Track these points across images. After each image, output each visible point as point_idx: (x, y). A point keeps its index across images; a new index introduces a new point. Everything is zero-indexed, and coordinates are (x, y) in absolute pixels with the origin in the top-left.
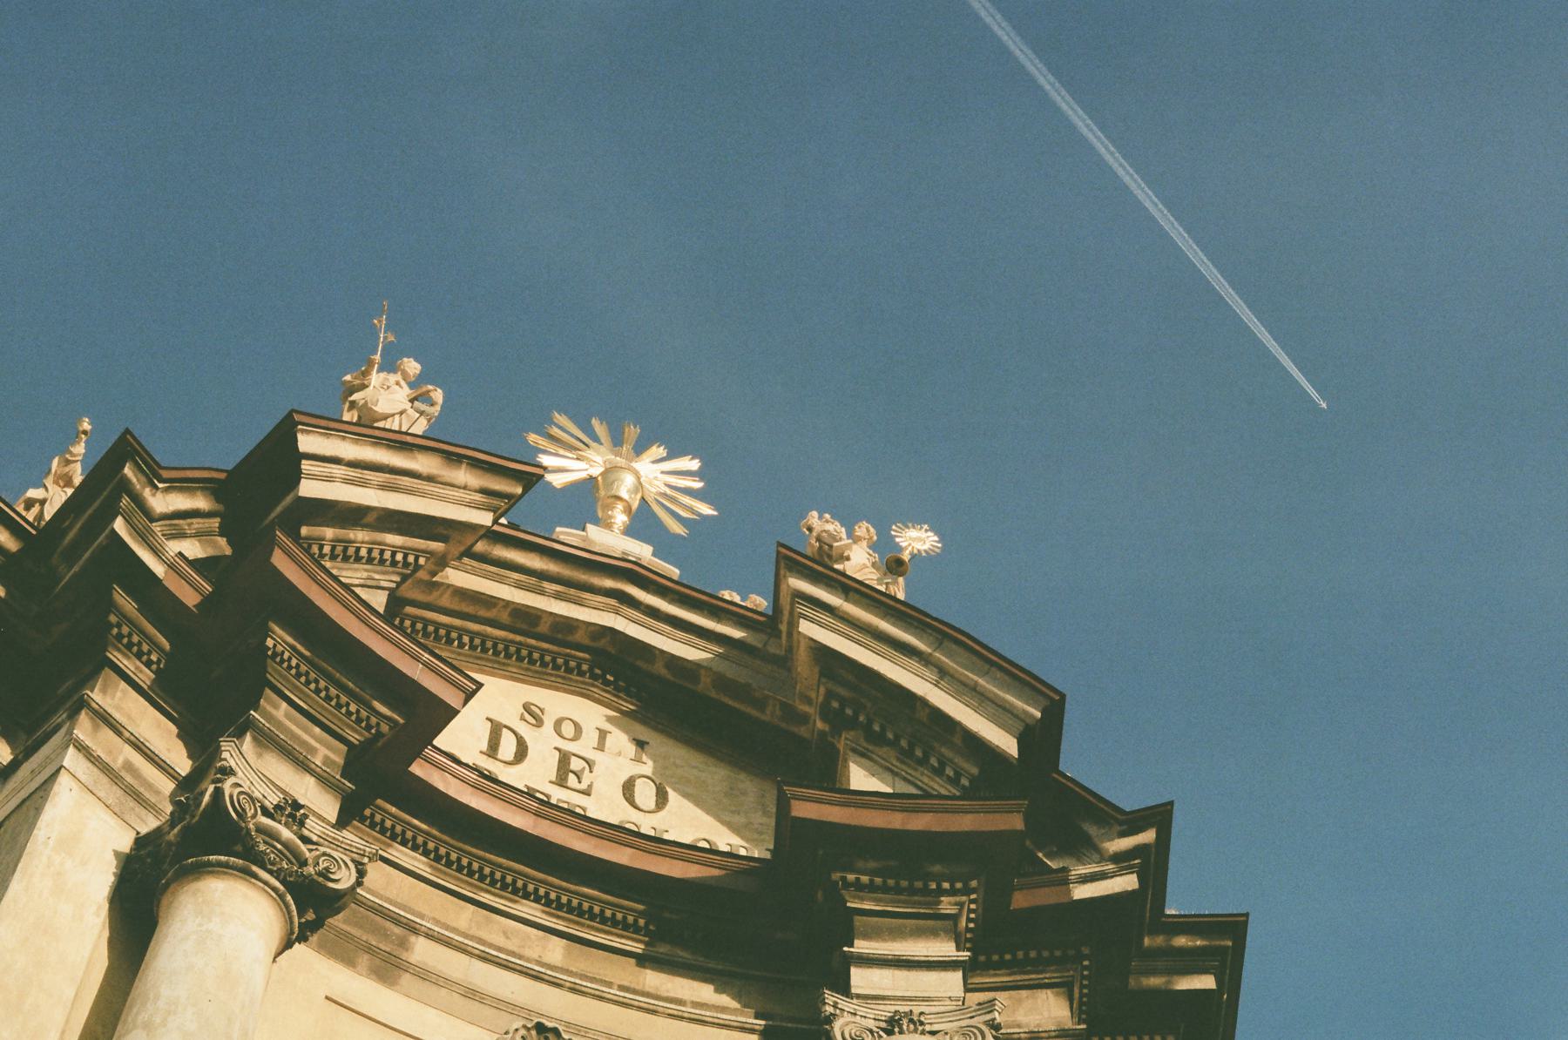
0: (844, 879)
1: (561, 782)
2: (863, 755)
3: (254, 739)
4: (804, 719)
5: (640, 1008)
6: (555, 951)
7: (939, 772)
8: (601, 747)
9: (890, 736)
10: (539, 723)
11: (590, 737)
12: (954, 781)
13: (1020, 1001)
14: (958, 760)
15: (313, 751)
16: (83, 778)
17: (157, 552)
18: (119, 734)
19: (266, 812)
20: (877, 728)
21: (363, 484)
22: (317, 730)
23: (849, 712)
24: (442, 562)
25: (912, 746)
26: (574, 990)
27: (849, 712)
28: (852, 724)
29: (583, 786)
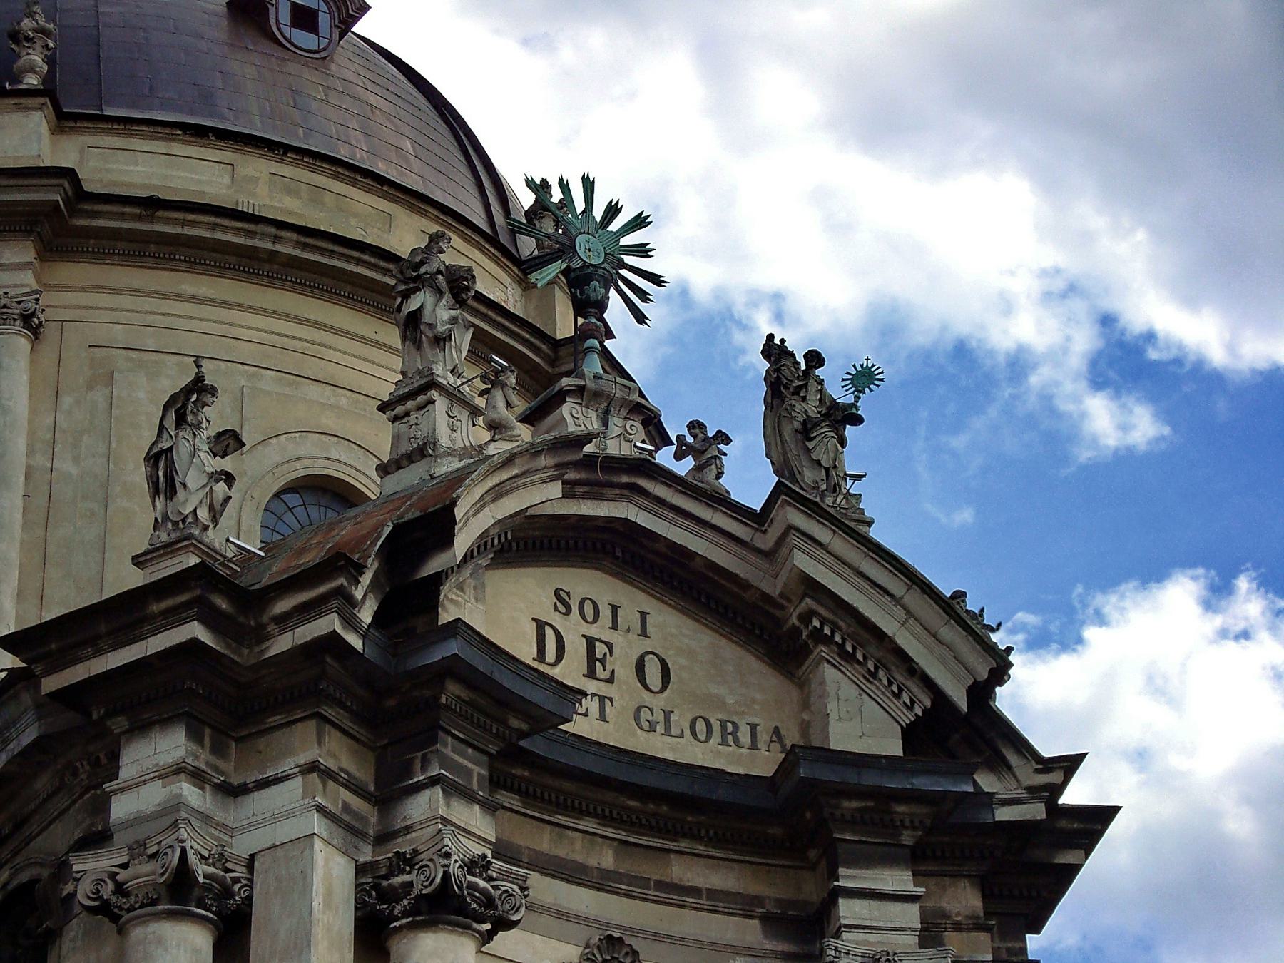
0: (832, 814)
1: (591, 674)
2: (835, 667)
3: (443, 790)
4: (782, 608)
5: (672, 905)
6: (606, 859)
8: (615, 626)
9: (861, 658)
10: (569, 610)
11: (606, 612)
12: (911, 708)
13: (944, 888)
14: (915, 690)
15: (469, 773)
16: (324, 835)
18: (336, 781)
20: (850, 650)
21: (483, 506)
22: (470, 750)
23: (827, 631)
25: (876, 668)
26: (627, 895)
27: (827, 631)
28: (828, 640)
29: (606, 675)
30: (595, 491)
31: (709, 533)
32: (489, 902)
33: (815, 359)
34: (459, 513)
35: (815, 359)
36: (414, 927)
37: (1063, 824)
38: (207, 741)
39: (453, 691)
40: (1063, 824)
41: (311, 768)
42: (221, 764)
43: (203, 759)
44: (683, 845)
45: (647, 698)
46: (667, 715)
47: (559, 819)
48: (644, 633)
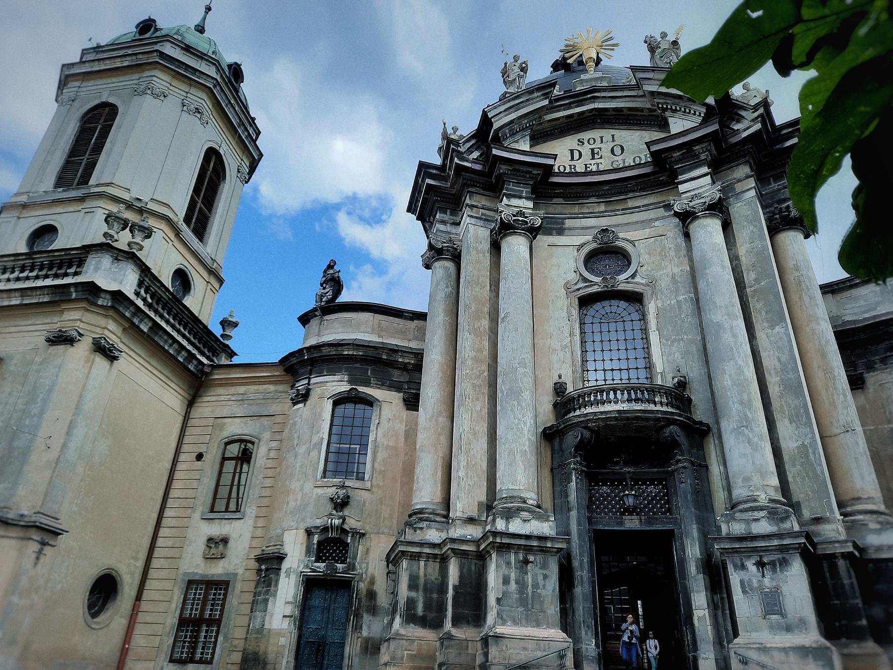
1: (593, 158)
4: (655, 110)
6: (602, 208)
7: (695, 114)
8: (602, 142)
10: (583, 143)
12: (700, 115)
17: (467, 161)
19: (514, 216)
24: (540, 117)
28: (667, 109)
30: (580, 103)
31: (624, 100)
32: (527, 223)
33: (664, 35)
34: (490, 115)
35: (664, 35)
36: (502, 238)
37: (785, 131)
38: (448, 213)
39: (503, 168)
40: (785, 131)
41: (467, 205)
42: (454, 218)
43: (447, 217)
44: (631, 195)
45: (616, 158)
46: (624, 161)
47: (580, 201)
48: (613, 140)
